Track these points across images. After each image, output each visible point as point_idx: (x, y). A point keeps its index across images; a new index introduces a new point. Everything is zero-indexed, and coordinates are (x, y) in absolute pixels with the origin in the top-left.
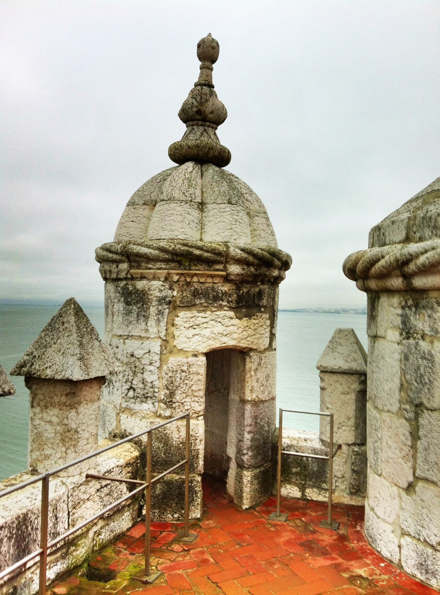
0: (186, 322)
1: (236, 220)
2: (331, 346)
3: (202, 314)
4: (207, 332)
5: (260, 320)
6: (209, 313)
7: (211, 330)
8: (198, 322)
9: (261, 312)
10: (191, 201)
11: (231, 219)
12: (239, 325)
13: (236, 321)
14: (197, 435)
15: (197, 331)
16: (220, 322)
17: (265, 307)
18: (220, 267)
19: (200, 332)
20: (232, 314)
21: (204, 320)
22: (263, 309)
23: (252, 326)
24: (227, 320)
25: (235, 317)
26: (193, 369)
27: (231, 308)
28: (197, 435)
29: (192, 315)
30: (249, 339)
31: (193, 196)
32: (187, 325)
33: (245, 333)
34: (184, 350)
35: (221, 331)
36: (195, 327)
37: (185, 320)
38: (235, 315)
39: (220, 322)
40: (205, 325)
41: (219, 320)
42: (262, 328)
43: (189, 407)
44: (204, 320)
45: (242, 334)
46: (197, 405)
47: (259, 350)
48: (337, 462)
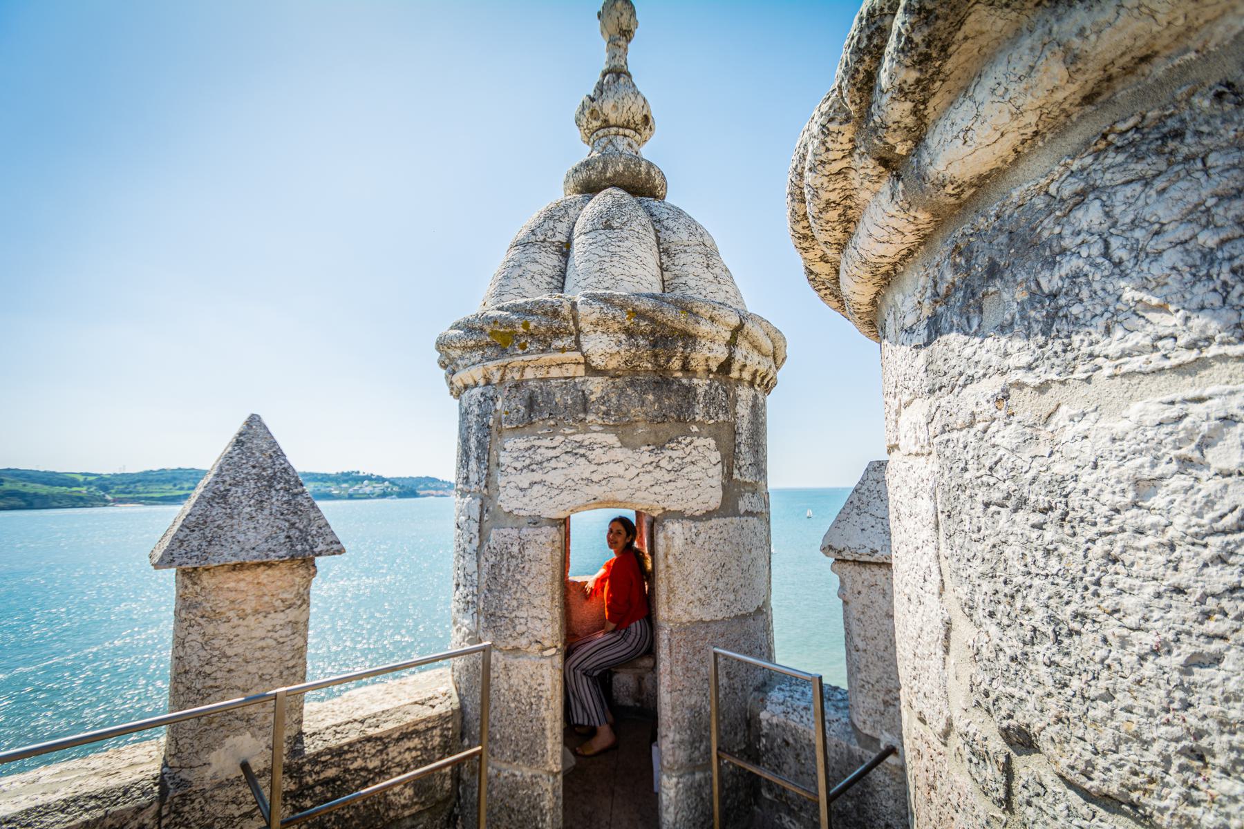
0: (517, 458)
1: (613, 254)
2: (856, 503)
3: (546, 442)
4: (556, 478)
5: (688, 450)
6: (559, 439)
7: (565, 471)
8: (539, 458)
9: (690, 434)
10: (545, 240)
11: (602, 254)
12: (630, 461)
13: (620, 454)
14: (543, 688)
15: (537, 476)
16: (583, 455)
17: (701, 424)
18: (567, 342)
19: (545, 477)
20: (611, 439)
21: (551, 453)
22: (695, 429)
23: (663, 463)
24: (598, 451)
25: (619, 444)
26: (531, 551)
27: (606, 428)
28: (543, 688)
29: (528, 445)
30: (657, 489)
31: (550, 233)
32: (519, 465)
33: (647, 479)
34: (515, 512)
35: (586, 475)
36: (534, 467)
37: (515, 455)
38: (620, 440)
39: (583, 455)
40: (553, 463)
41: (582, 451)
42: (694, 468)
43: (523, 628)
44: (551, 453)
45: (637, 480)
46: (538, 624)
47: (688, 513)
48: (890, 790)
